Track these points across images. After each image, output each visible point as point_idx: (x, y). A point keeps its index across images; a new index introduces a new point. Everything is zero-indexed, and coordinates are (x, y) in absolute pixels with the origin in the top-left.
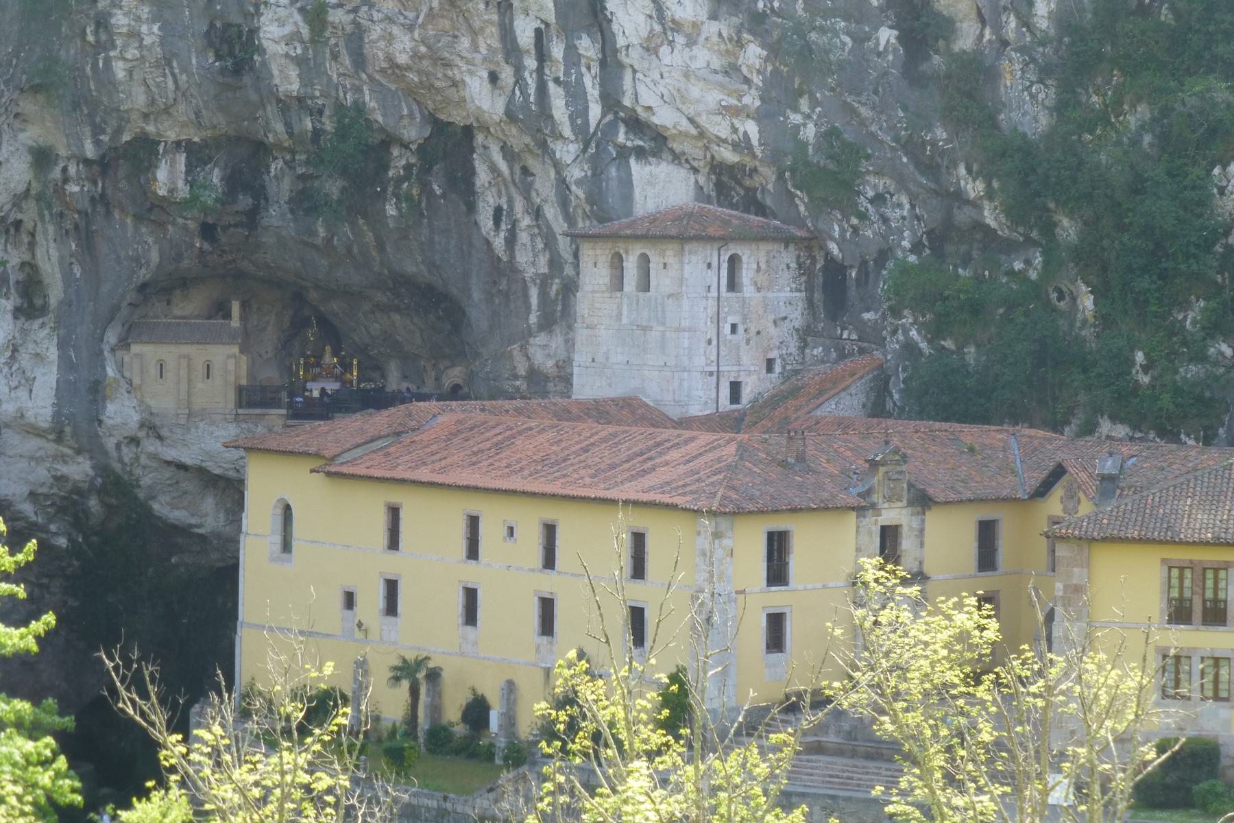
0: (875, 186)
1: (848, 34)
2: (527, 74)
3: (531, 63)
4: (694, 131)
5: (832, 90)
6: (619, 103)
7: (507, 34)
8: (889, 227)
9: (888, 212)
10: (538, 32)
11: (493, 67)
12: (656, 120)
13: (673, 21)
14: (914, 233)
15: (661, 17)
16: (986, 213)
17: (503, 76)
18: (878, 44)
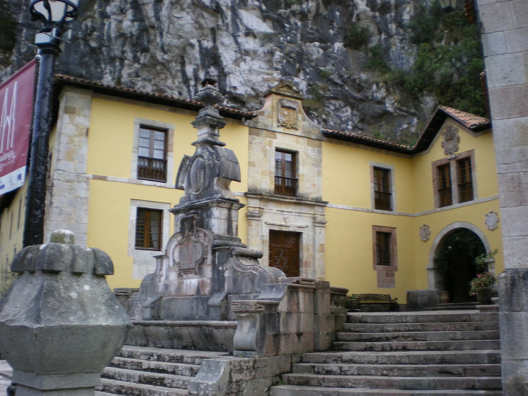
0: (334, 105)
1: (320, 47)
2: (191, 88)
3: (192, 83)
4: (253, 93)
5: (314, 67)
6: (225, 90)
7: (184, 73)
8: (341, 120)
9: (341, 115)
10: (194, 69)
11: (180, 90)
12: (238, 92)
13: (245, 51)
14: (353, 122)
15: (240, 50)
16: (387, 105)
17: (183, 93)
18: (334, 50)
